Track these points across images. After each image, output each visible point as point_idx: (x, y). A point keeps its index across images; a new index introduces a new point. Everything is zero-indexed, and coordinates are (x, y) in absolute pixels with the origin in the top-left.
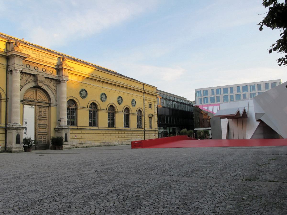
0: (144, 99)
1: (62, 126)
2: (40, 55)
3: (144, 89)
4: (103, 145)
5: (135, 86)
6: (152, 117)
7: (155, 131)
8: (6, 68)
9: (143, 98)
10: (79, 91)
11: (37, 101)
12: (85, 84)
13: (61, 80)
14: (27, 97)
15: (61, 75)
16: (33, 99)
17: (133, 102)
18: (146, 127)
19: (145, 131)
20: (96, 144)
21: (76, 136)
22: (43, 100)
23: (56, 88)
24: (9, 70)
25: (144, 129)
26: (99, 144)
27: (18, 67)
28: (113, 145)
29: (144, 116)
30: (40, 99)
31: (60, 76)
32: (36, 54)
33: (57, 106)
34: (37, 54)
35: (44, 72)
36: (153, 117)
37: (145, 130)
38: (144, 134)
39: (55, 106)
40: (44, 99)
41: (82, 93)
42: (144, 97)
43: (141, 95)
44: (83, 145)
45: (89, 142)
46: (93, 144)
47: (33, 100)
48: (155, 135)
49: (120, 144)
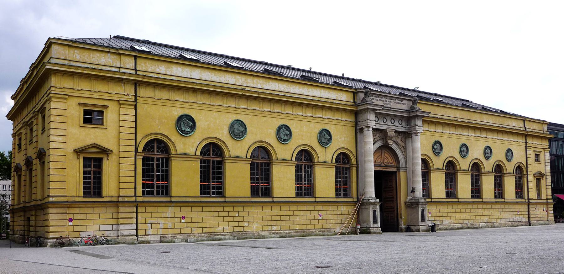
0: (526, 147)
1: (418, 199)
2: (388, 100)
3: (525, 128)
4: (465, 227)
5: (510, 124)
6: (541, 178)
7: (547, 203)
8: (354, 126)
9: (525, 145)
10: (431, 145)
11: (384, 165)
12: (439, 133)
13: (412, 132)
15: (412, 125)
17: (508, 154)
18: (530, 197)
19: (529, 204)
20: (455, 225)
23: (405, 144)
24: (358, 128)
25: (528, 199)
26: (460, 226)
27: (370, 124)
28: (480, 228)
29: (527, 177)
31: (411, 126)
32: (383, 101)
33: (406, 169)
34: (385, 100)
35: (393, 125)
36: (543, 177)
37: (530, 201)
38: (529, 208)
39: (405, 170)
40: (391, 162)
42: (526, 143)
43: (522, 140)
44: (439, 227)
45: (446, 222)
48: (546, 211)
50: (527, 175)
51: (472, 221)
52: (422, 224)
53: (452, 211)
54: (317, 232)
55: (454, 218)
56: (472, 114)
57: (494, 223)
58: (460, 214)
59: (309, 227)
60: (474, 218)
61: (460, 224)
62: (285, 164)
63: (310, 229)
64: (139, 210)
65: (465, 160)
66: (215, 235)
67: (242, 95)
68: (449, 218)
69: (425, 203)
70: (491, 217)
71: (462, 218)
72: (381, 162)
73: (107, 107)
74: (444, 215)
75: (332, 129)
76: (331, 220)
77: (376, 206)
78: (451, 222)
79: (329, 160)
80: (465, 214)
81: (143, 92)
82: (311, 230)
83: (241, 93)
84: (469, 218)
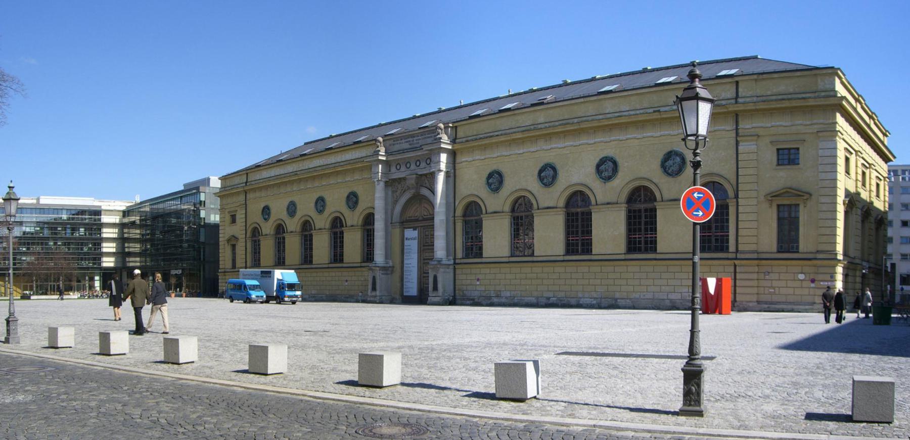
10: (484, 179)
12: (498, 158)
14: (410, 215)
20: (524, 300)
21: (478, 280)
22: (430, 215)
25: (737, 251)
30: (426, 214)
32: (409, 141)
41: (490, 181)
45: (508, 294)
65: (551, 189)
75: (355, 189)
79: (355, 223)
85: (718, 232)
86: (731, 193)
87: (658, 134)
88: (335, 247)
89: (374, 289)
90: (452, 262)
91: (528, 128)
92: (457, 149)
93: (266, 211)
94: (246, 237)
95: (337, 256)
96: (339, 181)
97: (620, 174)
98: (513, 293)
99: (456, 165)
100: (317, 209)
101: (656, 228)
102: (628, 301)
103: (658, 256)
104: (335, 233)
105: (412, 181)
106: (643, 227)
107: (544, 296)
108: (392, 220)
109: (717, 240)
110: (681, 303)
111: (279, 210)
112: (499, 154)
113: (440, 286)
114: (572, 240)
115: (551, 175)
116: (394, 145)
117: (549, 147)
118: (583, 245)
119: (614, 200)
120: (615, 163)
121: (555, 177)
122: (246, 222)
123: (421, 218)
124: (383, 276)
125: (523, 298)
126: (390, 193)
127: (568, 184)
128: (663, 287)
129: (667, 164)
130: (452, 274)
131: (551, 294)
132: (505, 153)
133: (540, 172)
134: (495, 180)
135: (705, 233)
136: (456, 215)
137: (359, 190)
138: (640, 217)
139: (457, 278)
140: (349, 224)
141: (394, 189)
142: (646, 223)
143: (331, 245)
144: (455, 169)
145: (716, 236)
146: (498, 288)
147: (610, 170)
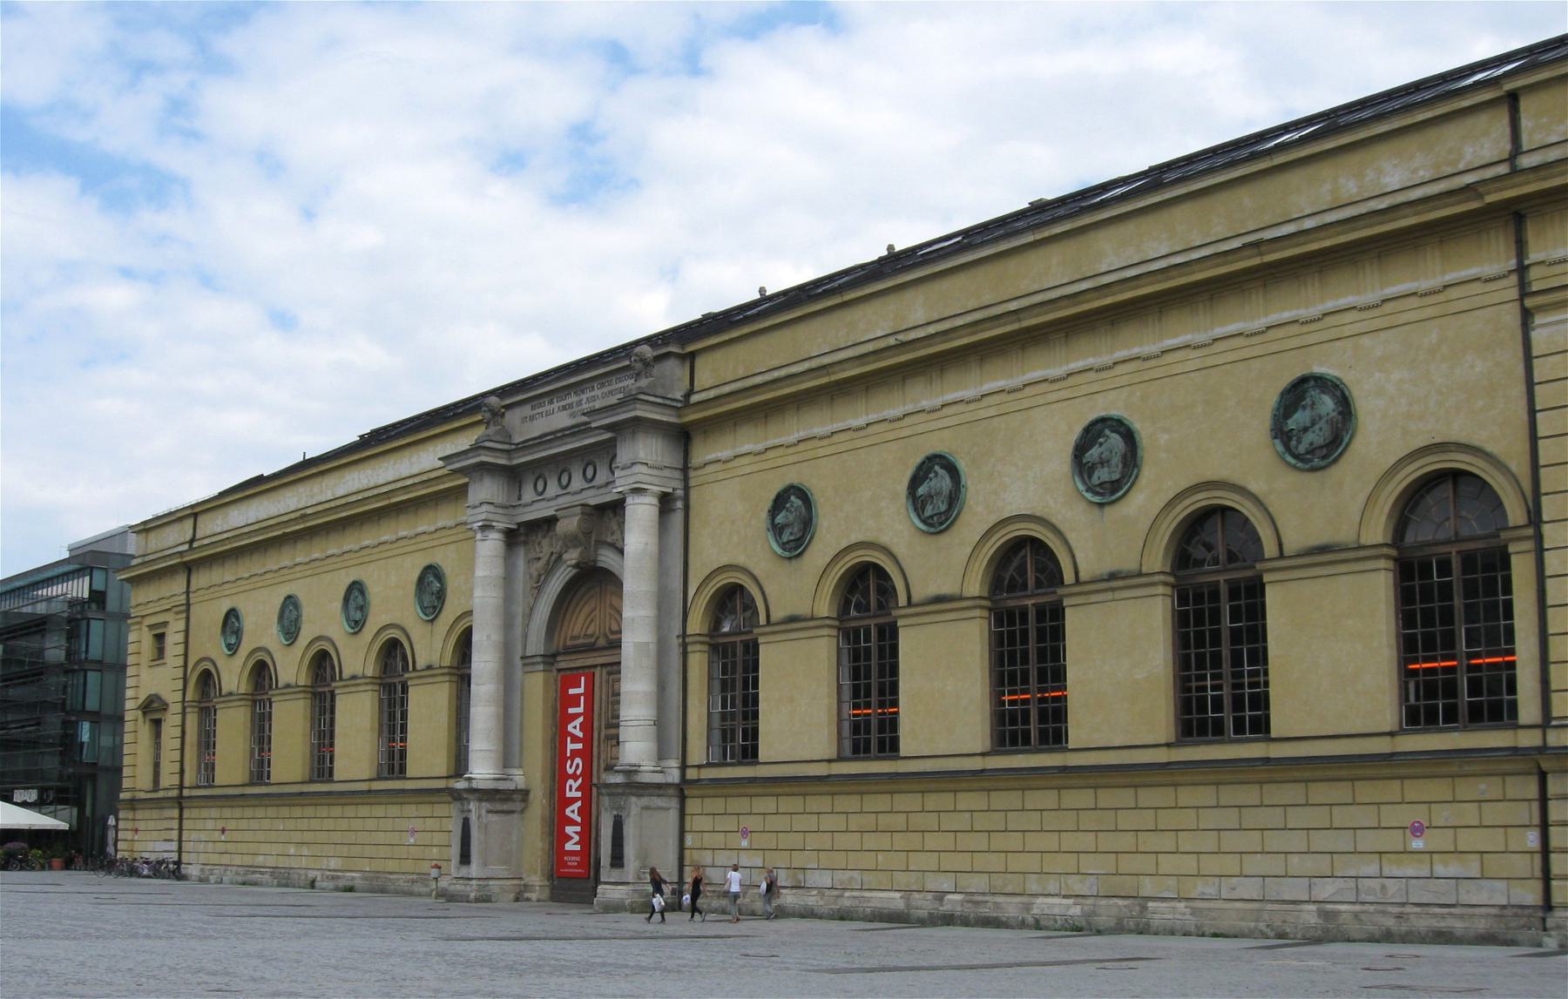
2: (584, 397)
4: (923, 913)
12: (801, 447)
14: (575, 633)
16: (592, 636)
20: (869, 899)
21: (745, 833)
25: (1546, 721)
26: (894, 900)
28: (1023, 925)
32: (571, 406)
41: (779, 519)
45: (824, 879)
46: (847, 894)
47: (593, 640)
49: (1108, 911)
50: (1530, 531)
51: (978, 883)
52: (608, 877)
53: (856, 822)
54: (401, 883)
55: (868, 860)
56: (1012, 264)
57: (1150, 904)
58: (900, 841)
59: (391, 866)
60: (995, 862)
61: (898, 895)
62: (353, 689)
63: (391, 873)
64: (186, 814)
65: (944, 539)
66: (254, 872)
67: (285, 534)
68: (839, 859)
69: (620, 790)
70: (1129, 864)
71: (917, 861)
72: (597, 633)
73: (165, 624)
74: (813, 841)
75: (437, 557)
76: (435, 850)
77: (469, 804)
78: (851, 879)
80: (932, 842)
81: (201, 579)
82: (392, 877)
83: (279, 533)
84: (961, 861)
85: (1477, 655)
86: (1515, 513)
87: (1260, 323)
88: (392, 730)
89: (465, 858)
90: (674, 776)
91: (882, 344)
92: (693, 423)
93: (231, 623)
94: (184, 700)
95: (394, 762)
96: (402, 533)
97: (1147, 473)
98: (839, 875)
99: (692, 474)
100: (348, 620)
101: (1265, 650)
102: (1181, 905)
103: (1276, 751)
104: (388, 688)
105: (569, 524)
106: (1225, 651)
107: (929, 887)
108: (525, 649)
109: (1475, 688)
110: (1356, 915)
111: (261, 630)
112: (802, 434)
113: (630, 850)
114: (1012, 703)
115: (946, 491)
116: (532, 418)
117: (938, 401)
118: (1043, 717)
119: (1130, 565)
120: (1129, 436)
121: (955, 497)
122: (186, 655)
123: (602, 642)
124: (494, 818)
125: (867, 894)
126: (521, 563)
127: (993, 519)
128: (1295, 859)
129: (1292, 424)
130: (673, 816)
131: (946, 883)
132: (818, 430)
133: (915, 482)
134: (791, 518)
135: (1434, 659)
136: (689, 631)
137: (445, 559)
138: (1216, 617)
139: (688, 828)
140: (421, 664)
141: (533, 555)
142: (1236, 636)
143: (381, 725)
144: (687, 488)
145: (1471, 668)
146: (799, 859)
147: (1116, 460)
